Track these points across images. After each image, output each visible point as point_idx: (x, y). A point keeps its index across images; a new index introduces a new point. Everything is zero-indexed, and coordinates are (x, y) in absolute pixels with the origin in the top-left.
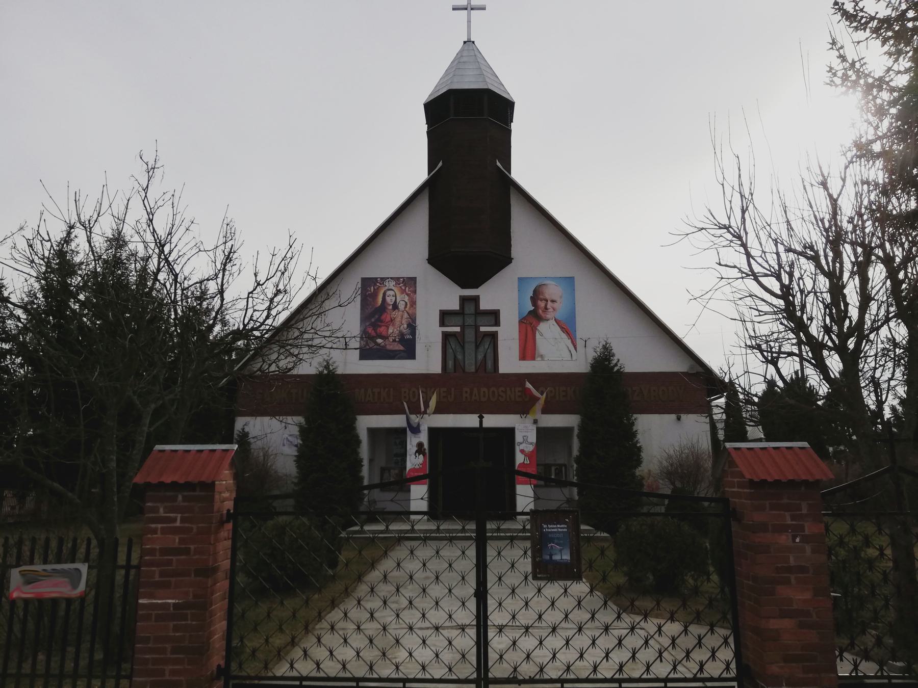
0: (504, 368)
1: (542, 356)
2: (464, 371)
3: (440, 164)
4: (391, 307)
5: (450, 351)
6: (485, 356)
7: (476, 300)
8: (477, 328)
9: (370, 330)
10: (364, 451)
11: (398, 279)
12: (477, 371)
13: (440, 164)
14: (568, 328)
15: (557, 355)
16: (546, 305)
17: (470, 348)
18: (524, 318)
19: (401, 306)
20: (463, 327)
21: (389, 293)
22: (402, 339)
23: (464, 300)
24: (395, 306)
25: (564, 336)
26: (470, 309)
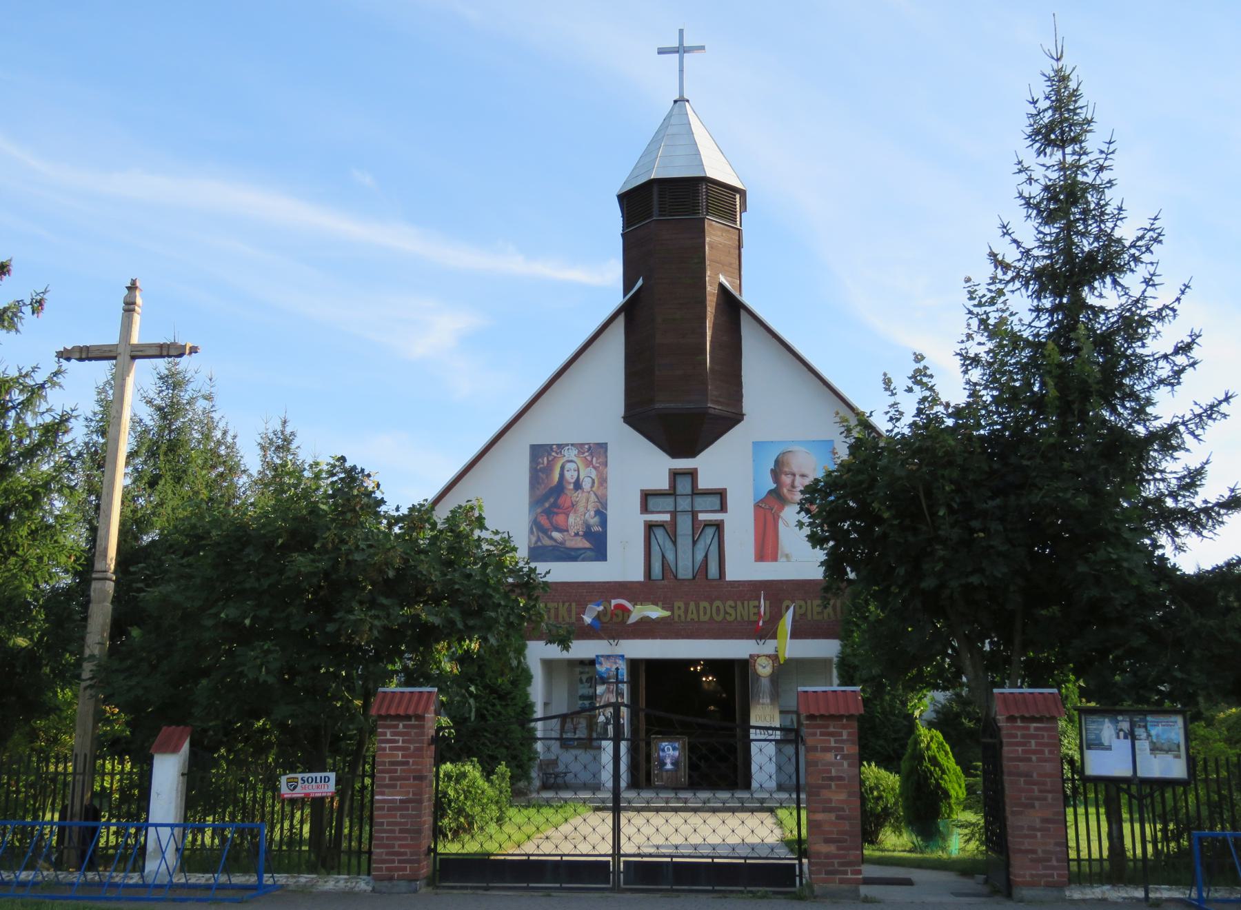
0: (732, 575)
1: (787, 556)
2: (676, 577)
3: (640, 283)
4: (571, 486)
5: (655, 549)
6: (706, 556)
7: (692, 474)
8: (694, 514)
9: (543, 521)
10: (537, 692)
11: (582, 445)
12: (694, 578)
13: (640, 283)
16: (793, 482)
17: (684, 541)
18: (762, 501)
19: (586, 484)
20: (674, 514)
21: (568, 466)
22: (588, 534)
23: (675, 475)
24: (578, 485)
26: (684, 486)
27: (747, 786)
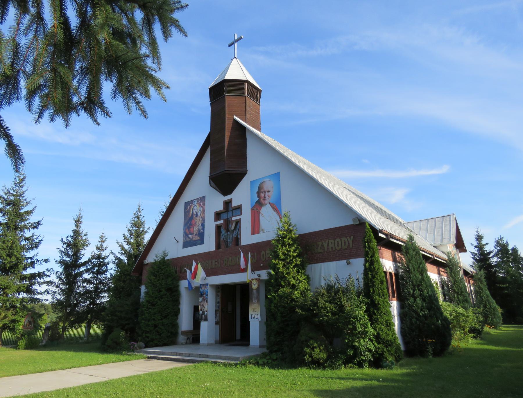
9: (187, 231)
14: (277, 209)
15: (270, 228)
18: (254, 207)
19: (199, 215)
24: (197, 215)
25: (275, 213)
27: (248, 345)
